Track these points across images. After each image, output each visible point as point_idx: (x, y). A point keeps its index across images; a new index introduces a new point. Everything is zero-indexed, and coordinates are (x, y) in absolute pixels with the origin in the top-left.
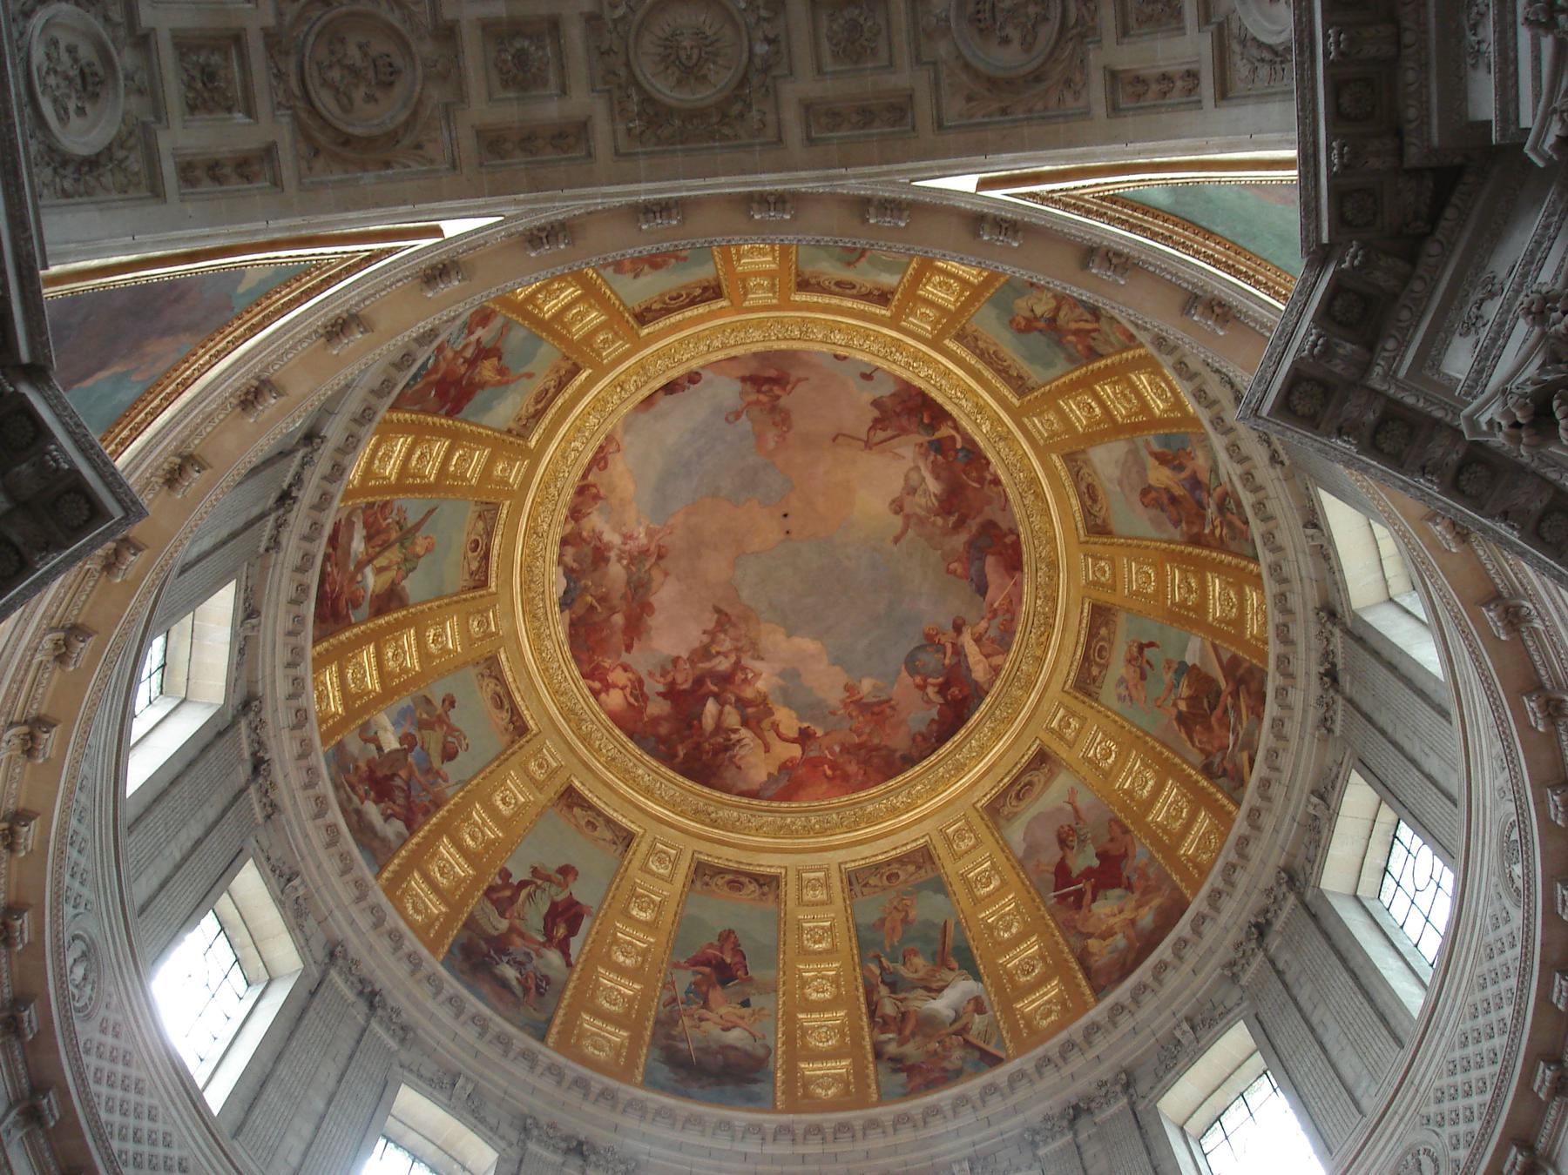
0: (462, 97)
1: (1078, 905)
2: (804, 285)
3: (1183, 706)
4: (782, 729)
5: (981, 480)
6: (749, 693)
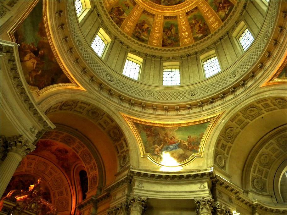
0: (271, 102)
2: (196, 8)
3: (120, 9)
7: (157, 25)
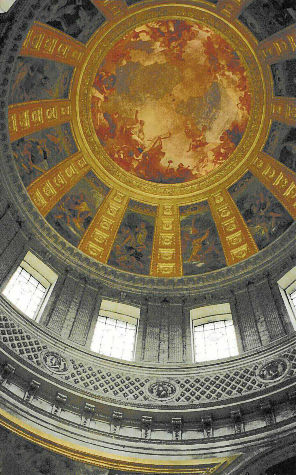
1: (32, 68)
4: (145, 34)
5: (123, 149)
6: (161, 39)
7: (108, 212)
